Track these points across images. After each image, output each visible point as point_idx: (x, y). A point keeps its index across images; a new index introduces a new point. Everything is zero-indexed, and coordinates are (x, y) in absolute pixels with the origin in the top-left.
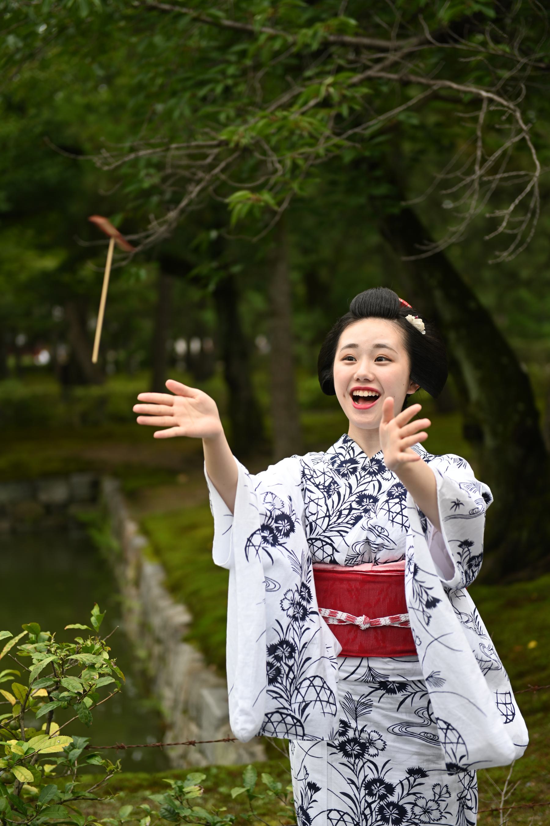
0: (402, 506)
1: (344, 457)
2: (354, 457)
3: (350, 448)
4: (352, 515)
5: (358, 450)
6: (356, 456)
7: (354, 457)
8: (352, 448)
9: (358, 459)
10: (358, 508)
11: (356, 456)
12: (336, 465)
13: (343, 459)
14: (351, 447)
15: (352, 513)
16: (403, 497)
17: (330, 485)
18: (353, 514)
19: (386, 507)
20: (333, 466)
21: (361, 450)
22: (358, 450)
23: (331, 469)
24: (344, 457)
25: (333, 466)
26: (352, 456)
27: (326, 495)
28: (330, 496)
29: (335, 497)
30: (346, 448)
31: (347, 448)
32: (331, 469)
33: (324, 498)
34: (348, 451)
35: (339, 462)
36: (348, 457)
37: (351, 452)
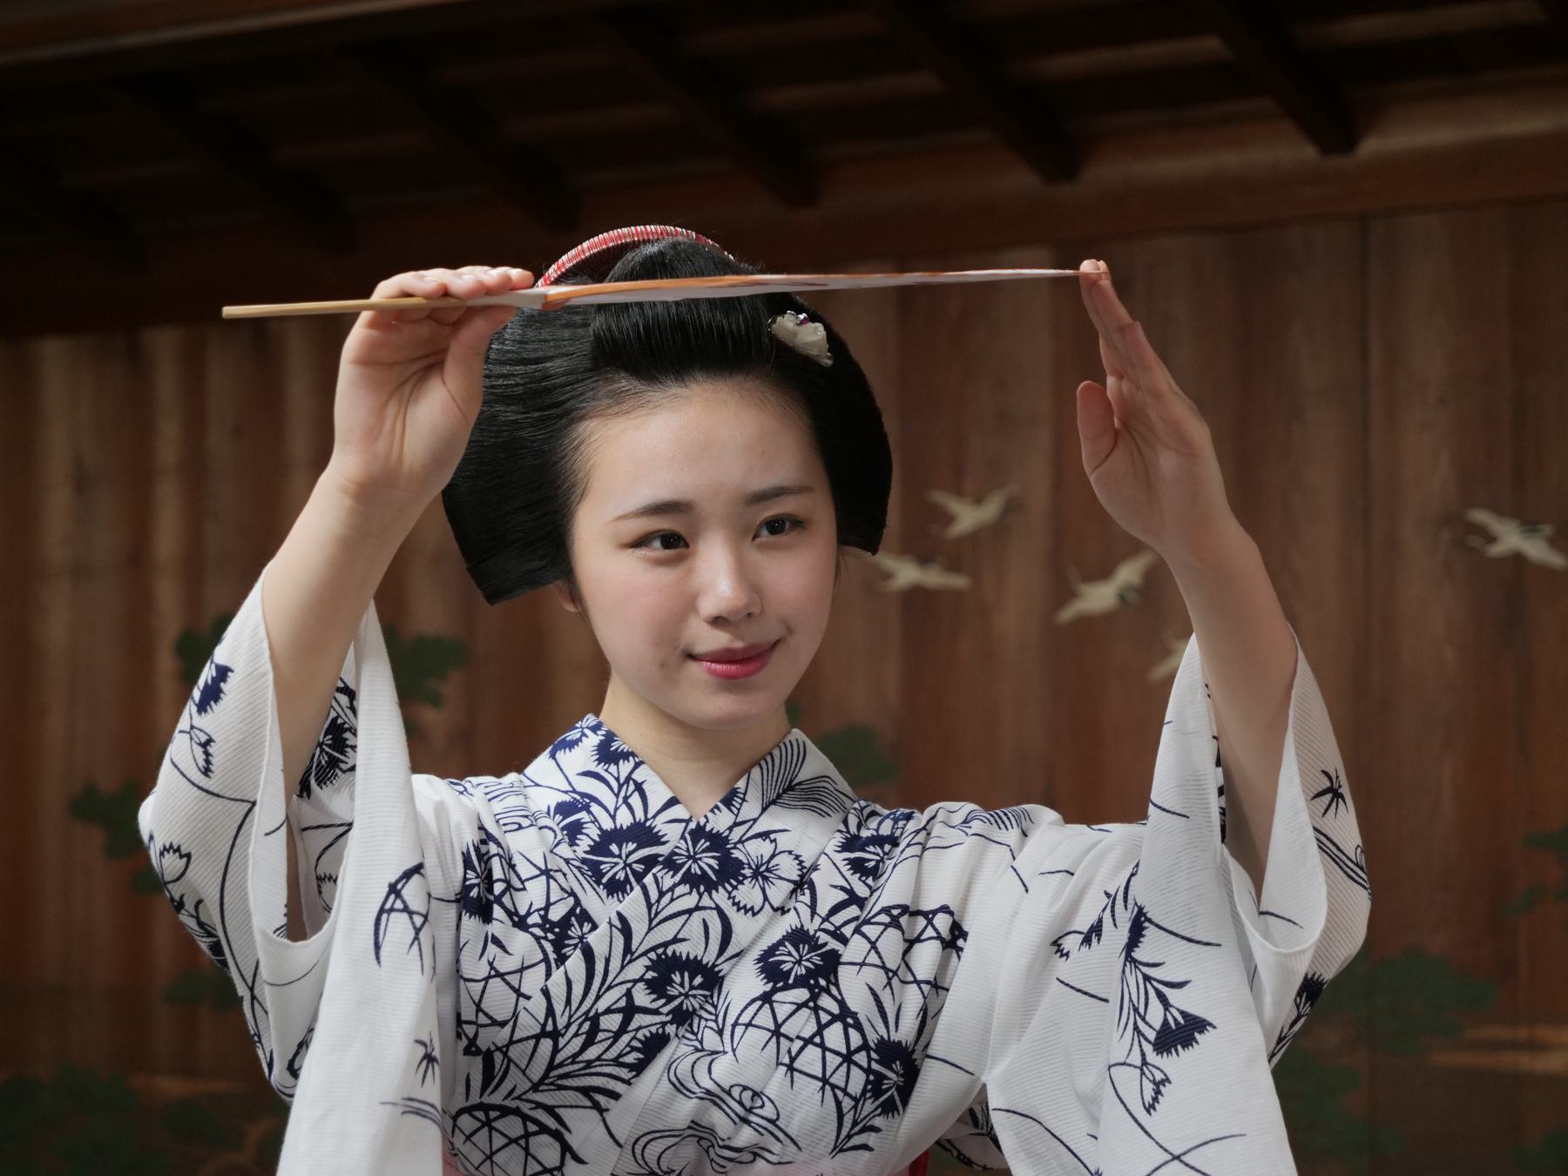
0: (821, 1013)
1: (613, 817)
2: (647, 819)
3: (632, 787)
4: (632, 1034)
5: (658, 794)
6: (654, 817)
7: (647, 819)
8: (639, 788)
9: (659, 825)
10: (655, 1005)
11: (654, 817)
12: (584, 843)
13: (607, 824)
14: (635, 783)
15: (633, 1025)
16: (823, 982)
17: (565, 923)
18: (637, 1030)
19: (765, 1018)
20: (572, 843)
21: (668, 795)
22: (658, 794)
23: (567, 861)
24: (613, 817)
25: (572, 843)
26: (640, 815)
27: (552, 956)
28: (562, 959)
29: (576, 963)
30: (615, 785)
31: (620, 787)
32: (567, 861)
33: (542, 966)
34: (626, 799)
35: (594, 832)
36: (624, 819)
37: (635, 800)
